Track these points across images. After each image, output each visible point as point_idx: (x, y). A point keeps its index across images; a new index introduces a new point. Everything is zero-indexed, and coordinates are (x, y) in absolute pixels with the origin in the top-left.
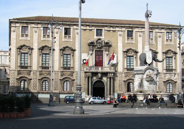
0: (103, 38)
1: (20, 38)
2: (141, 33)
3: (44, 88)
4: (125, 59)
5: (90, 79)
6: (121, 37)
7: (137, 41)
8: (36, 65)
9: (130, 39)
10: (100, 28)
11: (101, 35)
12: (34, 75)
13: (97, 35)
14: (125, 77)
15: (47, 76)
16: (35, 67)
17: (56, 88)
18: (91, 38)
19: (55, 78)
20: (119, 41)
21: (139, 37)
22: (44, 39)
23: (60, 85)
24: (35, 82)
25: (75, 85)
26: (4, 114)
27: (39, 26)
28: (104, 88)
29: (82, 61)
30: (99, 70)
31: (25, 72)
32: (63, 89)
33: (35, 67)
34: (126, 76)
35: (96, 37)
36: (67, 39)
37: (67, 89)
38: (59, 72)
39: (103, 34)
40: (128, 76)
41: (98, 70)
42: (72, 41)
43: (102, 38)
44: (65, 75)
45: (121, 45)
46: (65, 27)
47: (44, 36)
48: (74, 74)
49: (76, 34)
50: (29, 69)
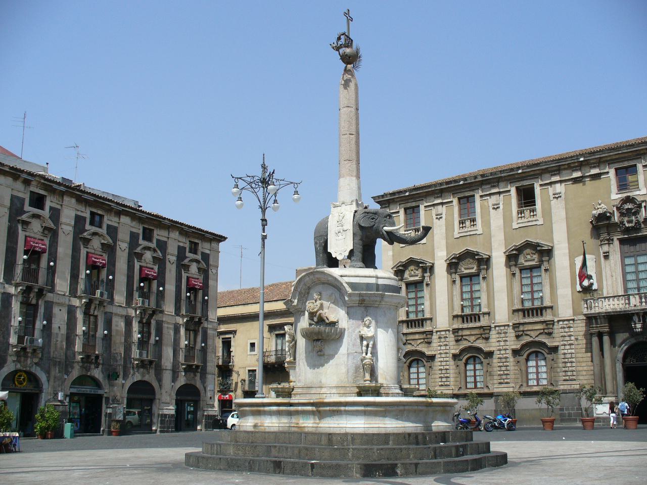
3: (472, 379)
5: (606, 339)
10: (626, 164)
12: (441, 344)
16: (442, 321)
18: (600, 202)
23: (516, 368)
24: (444, 364)
31: (417, 337)
32: (524, 380)
36: (526, 220)
37: (538, 379)
38: (508, 326)
42: (541, 222)
44: (528, 333)
46: (519, 184)
47: (462, 222)
48: (557, 330)
50: (427, 327)
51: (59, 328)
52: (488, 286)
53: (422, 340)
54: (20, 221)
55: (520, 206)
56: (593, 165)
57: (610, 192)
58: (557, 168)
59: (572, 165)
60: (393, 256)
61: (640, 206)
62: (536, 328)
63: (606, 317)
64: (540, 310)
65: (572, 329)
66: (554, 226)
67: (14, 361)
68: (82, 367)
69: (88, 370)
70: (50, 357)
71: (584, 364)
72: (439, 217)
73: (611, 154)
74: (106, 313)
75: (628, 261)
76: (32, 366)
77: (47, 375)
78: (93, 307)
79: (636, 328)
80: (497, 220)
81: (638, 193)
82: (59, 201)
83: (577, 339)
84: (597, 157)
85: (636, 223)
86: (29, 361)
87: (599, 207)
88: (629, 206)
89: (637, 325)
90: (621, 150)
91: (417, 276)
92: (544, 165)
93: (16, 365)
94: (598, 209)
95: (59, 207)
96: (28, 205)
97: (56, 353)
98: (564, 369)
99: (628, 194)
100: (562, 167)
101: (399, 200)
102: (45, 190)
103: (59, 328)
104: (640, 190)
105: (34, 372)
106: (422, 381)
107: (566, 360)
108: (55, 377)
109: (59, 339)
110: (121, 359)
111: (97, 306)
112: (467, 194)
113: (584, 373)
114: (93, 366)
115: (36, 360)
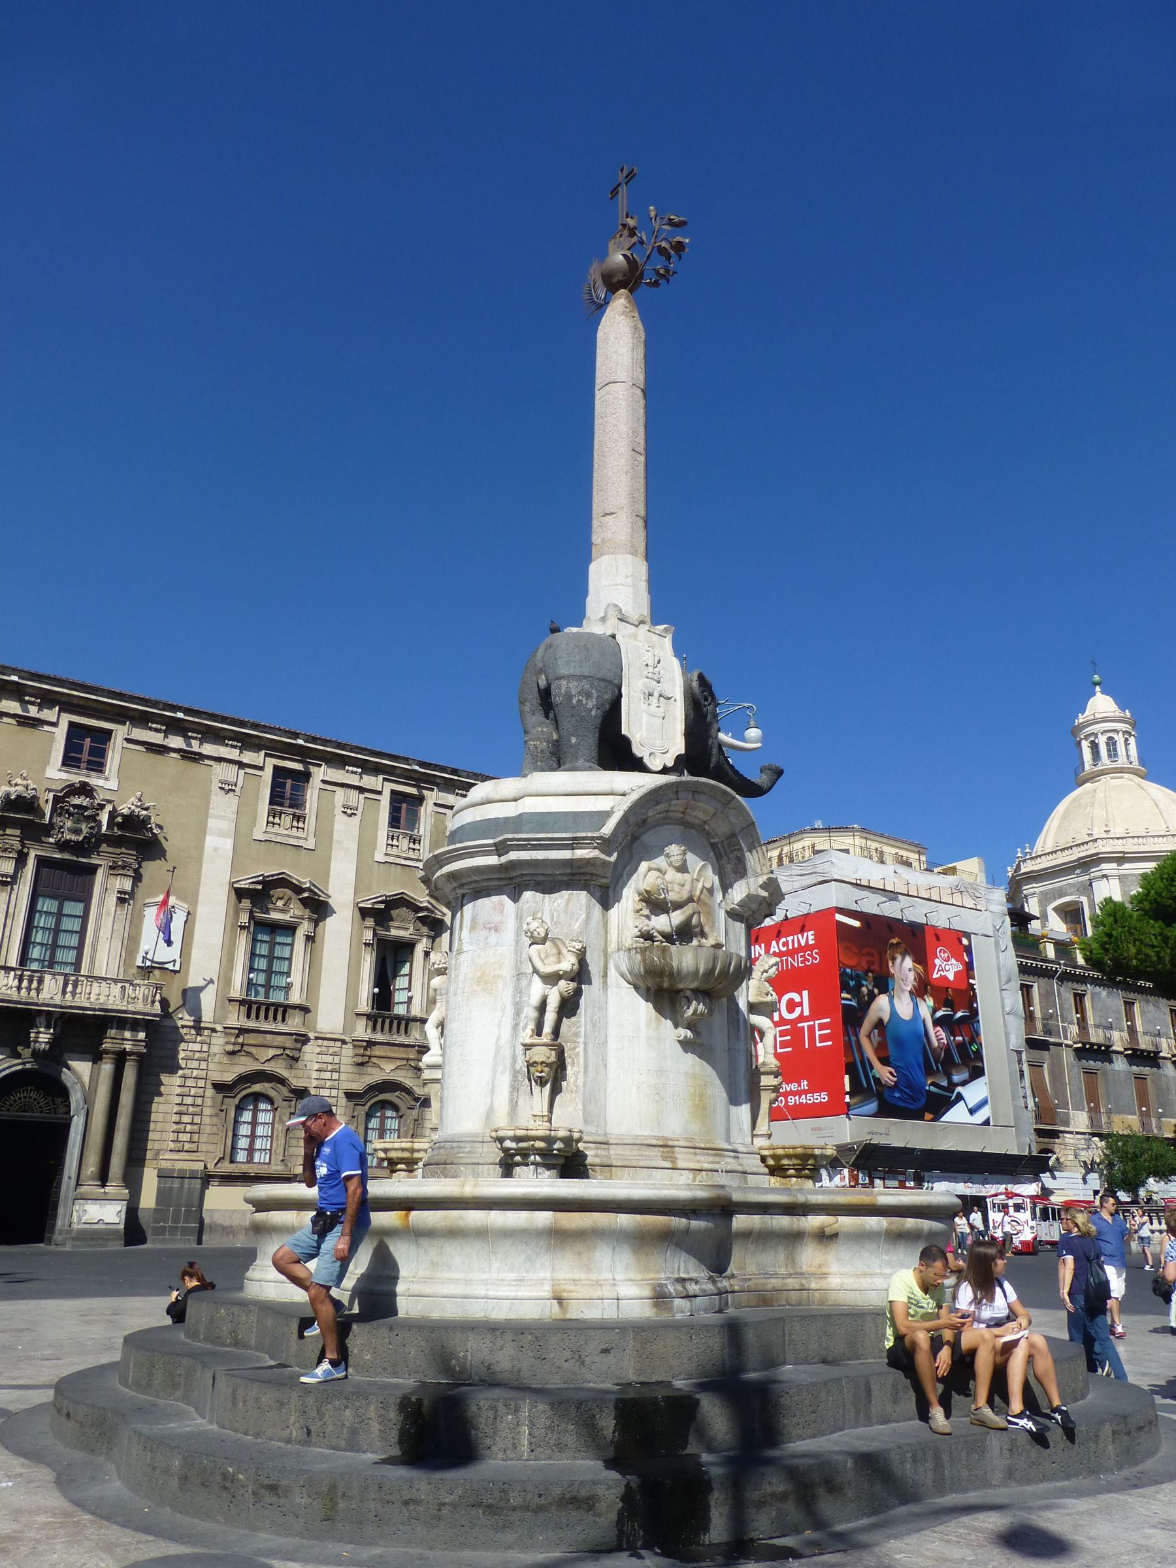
0: (113, 784)
2: (354, 797)
4: (243, 941)
6: (232, 799)
7: (325, 835)
9: (287, 820)
11: (97, 766)
13: (69, 761)
14: (225, 1059)
20: (211, 823)
21: (340, 818)
28: (65, 1127)
34: (233, 1053)
35: (56, 774)
39: (113, 759)
40: (249, 1054)
41: (38, 990)
43: (106, 783)
45: (228, 844)
57: (46, 762)
75: (46, 905)
79: (36, 1042)
81: (100, 782)
85: (85, 837)
87: (19, 781)
89: (41, 1035)
94: (16, 785)
99: (87, 780)
104: (106, 779)
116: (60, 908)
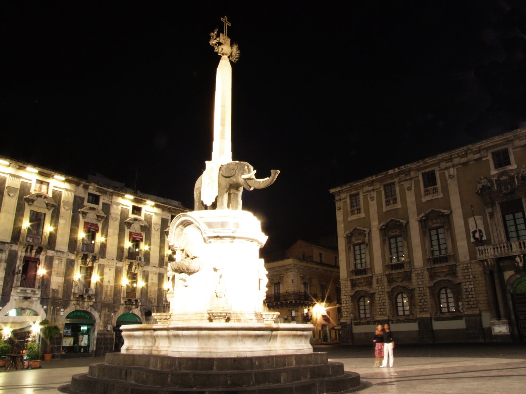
1: (350, 219)
5: (496, 275)
8: (381, 263)
11: (508, 163)
12: (379, 285)
13: (498, 165)
15: (405, 284)
16: (378, 268)
17: (424, 307)
19: (418, 286)
22: (389, 208)
24: (381, 299)
25: (464, 296)
26: (29, 362)
27: (377, 186)
29: (472, 235)
30: (514, 250)
33: (378, 268)
39: (512, 158)
41: (511, 249)
42: (441, 196)
44: (438, 274)
49: (447, 179)
51: (109, 281)
52: (408, 243)
53: (366, 283)
54: (81, 212)
55: (425, 186)
56: (475, 153)
57: (489, 170)
58: (450, 157)
59: (460, 154)
60: (344, 227)
61: (512, 178)
62: (443, 270)
63: (494, 259)
64: (445, 259)
65: (470, 270)
66: (451, 197)
67: (74, 304)
68: (126, 308)
69: (130, 309)
70: (102, 301)
71: (481, 295)
72: (372, 199)
73: (488, 143)
74: (144, 272)
75: (509, 217)
76: (88, 307)
77: (99, 313)
78: (134, 267)
80: (411, 198)
82: (109, 199)
83: (474, 277)
84: (477, 146)
86: (86, 304)
88: (504, 178)
90: (494, 139)
91: (360, 239)
92: (441, 156)
93: (76, 307)
95: (109, 203)
96: (87, 201)
97: (106, 298)
98: (467, 300)
100: (453, 156)
101: (345, 190)
102: (100, 192)
103: (109, 281)
105: (89, 311)
106: (368, 311)
107: (468, 293)
108: (105, 315)
109: (109, 289)
110: (155, 302)
111: (137, 267)
112: (389, 182)
113: (482, 302)
114: (134, 307)
115: (91, 303)
116: (514, 216)
